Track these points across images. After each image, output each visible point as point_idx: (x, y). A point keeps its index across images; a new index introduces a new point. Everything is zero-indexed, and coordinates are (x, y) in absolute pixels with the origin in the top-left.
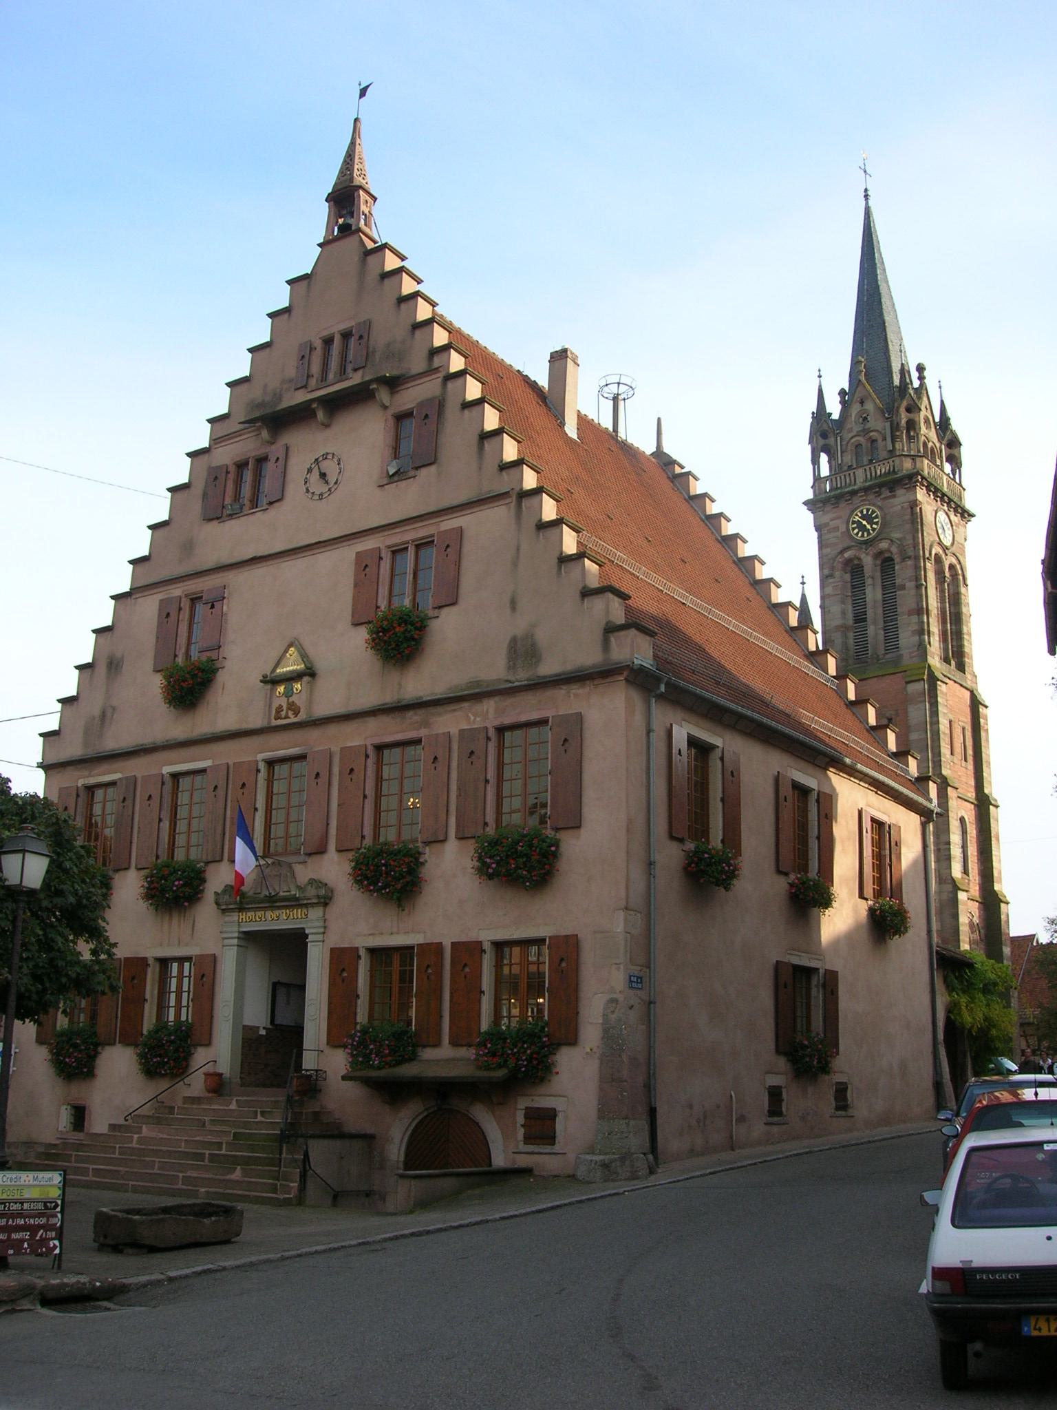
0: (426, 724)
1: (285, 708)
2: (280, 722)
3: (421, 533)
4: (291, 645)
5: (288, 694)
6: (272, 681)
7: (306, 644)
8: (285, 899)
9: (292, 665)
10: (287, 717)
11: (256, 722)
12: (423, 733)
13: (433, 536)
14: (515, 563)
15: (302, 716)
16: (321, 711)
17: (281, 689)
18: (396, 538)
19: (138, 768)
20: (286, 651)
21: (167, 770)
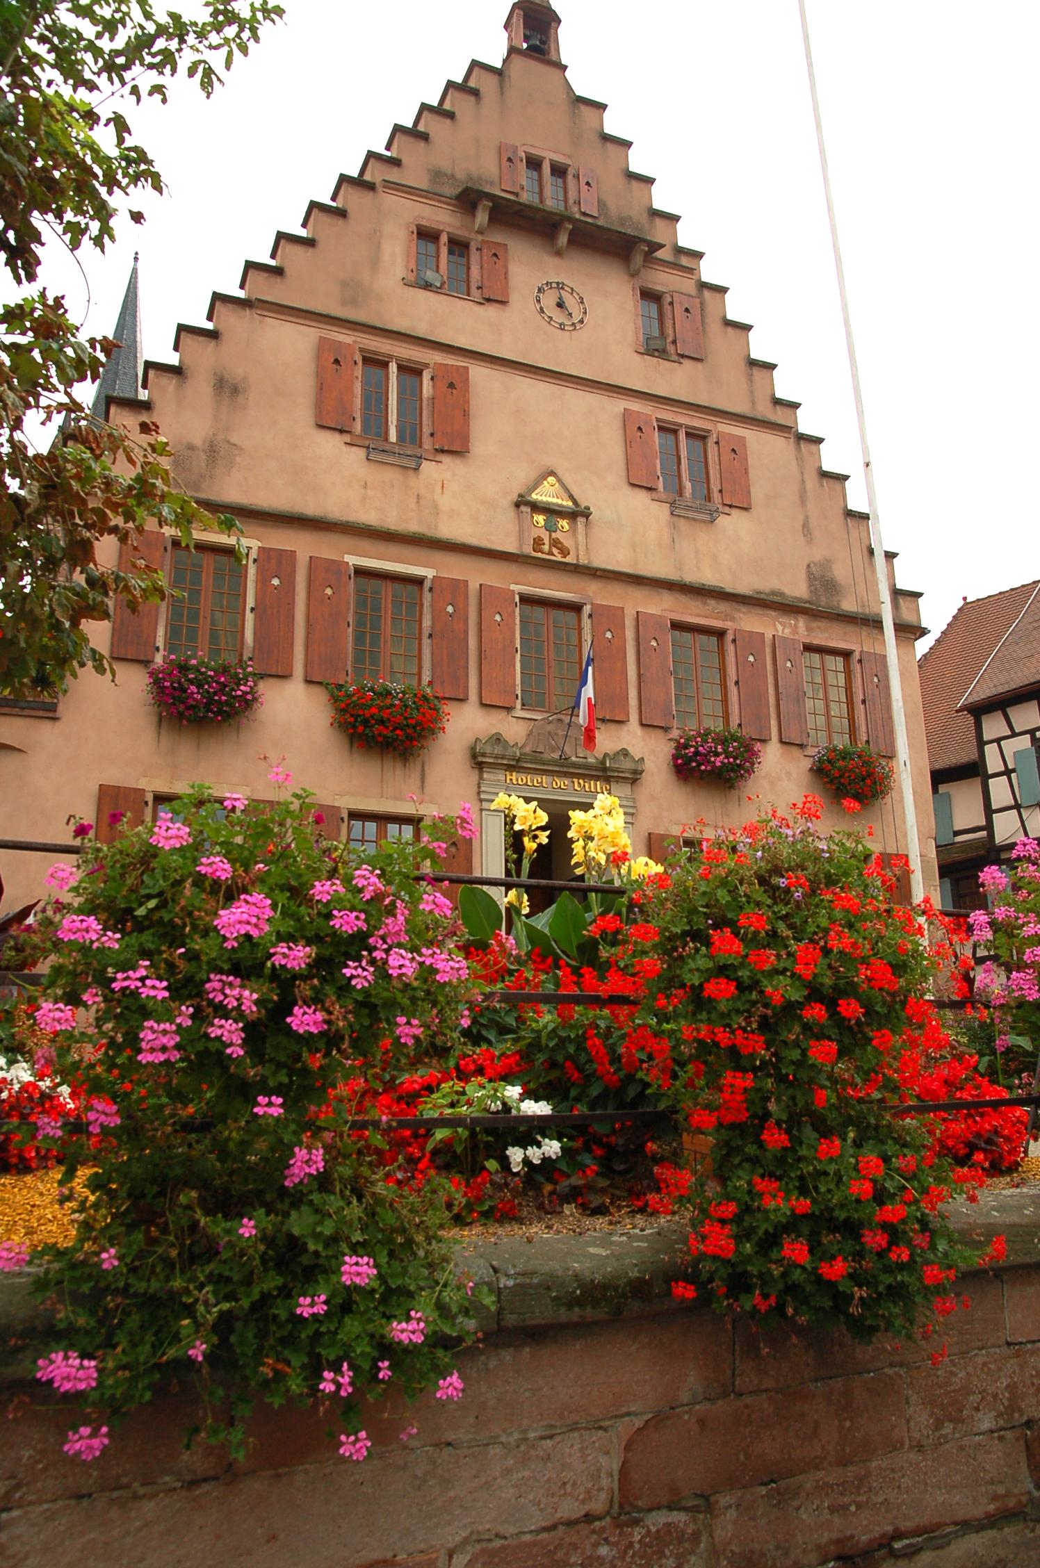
0: (732, 619)
1: (546, 541)
2: (539, 555)
3: (697, 423)
4: (552, 473)
5: (550, 528)
6: (523, 503)
7: (568, 480)
8: (580, 766)
9: (547, 494)
10: (550, 553)
11: (511, 548)
12: (727, 625)
13: (709, 431)
14: (803, 499)
15: (567, 560)
16: (599, 561)
17: (540, 519)
18: (668, 415)
19: (303, 546)
20: (544, 477)
21: (353, 560)
